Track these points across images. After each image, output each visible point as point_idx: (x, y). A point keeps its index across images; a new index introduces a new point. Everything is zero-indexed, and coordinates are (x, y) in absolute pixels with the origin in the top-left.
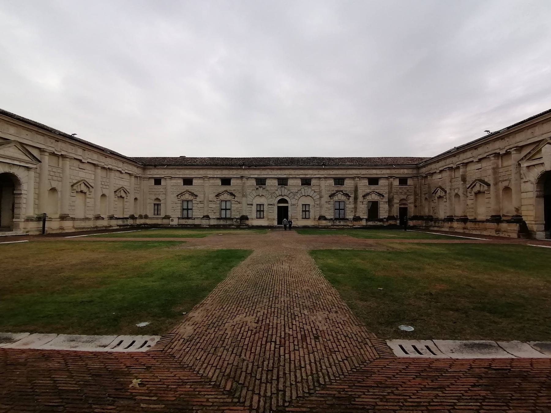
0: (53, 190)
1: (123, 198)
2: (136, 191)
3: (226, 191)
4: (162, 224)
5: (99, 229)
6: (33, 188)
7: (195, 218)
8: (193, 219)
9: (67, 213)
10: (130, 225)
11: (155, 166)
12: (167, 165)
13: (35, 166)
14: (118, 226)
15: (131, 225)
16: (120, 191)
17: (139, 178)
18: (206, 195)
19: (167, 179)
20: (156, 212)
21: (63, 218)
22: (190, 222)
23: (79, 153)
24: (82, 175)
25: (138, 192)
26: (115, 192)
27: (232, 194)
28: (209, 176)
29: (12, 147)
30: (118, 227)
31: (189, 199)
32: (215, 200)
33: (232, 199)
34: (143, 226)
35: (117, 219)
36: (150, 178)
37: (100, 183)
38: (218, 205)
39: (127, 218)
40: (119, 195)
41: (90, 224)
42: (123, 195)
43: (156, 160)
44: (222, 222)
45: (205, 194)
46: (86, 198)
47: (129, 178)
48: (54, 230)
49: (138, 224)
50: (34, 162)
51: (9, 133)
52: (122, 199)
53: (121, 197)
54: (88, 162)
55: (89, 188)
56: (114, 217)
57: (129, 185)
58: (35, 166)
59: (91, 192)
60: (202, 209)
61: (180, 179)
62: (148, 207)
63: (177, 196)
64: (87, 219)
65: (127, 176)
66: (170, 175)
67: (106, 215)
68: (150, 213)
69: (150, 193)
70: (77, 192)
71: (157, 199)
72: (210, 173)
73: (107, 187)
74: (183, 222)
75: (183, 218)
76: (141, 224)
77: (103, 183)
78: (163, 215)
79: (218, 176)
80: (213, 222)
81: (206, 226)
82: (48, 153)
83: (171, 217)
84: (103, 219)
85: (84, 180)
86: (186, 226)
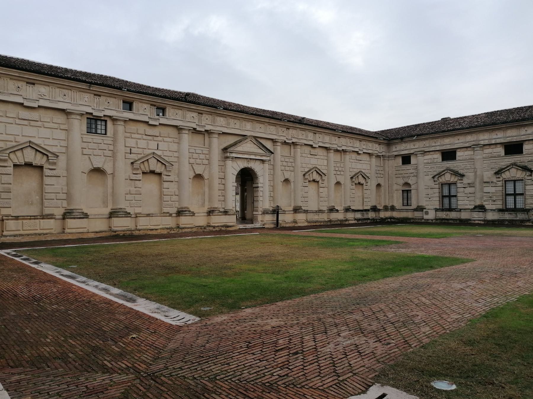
0: (287, 181)
1: (362, 184)
2: (379, 175)
3: (514, 165)
4: (413, 219)
5: (333, 223)
6: (268, 180)
7: (461, 209)
8: (458, 211)
9: (299, 205)
10: (371, 220)
11: (402, 139)
12: (418, 135)
13: (268, 158)
14: (355, 219)
15: (373, 219)
16: (358, 176)
17: (382, 159)
18: (478, 173)
19: (418, 156)
20: (405, 202)
21: (296, 210)
22: (453, 215)
23: (309, 137)
24: (314, 162)
25: (382, 176)
26: (352, 178)
27: (525, 168)
28: (482, 143)
29: (248, 142)
30: (356, 222)
31: (451, 181)
32: (495, 180)
33: (526, 177)
34: (389, 220)
35: (306, 212)
36: (396, 156)
37: (333, 168)
38: (500, 188)
39: (368, 210)
40: (357, 182)
41: (324, 217)
42: (362, 181)
43: (405, 130)
44: (507, 216)
45: (475, 172)
46: (319, 187)
47: (368, 159)
48: (287, 223)
49: (382, 218)
50: (268, 154)
51: (246, 129)
52: (360, 187)
53: (359, 183)
54: (319, 146)
55: (321, 175)
56: (351, 209)
57: (369, 168)
58: (268, 158)
59: (323, 180)
60: (472, 195)
61: (437, 152)
62: (395, 195)
63: (433, 177)
64: (320, 211)
65: (366, 157)
66: (423, 149)
67: (341, 206)
68: (398, 203)
69: (397, 176)
70: (309, 181)
71: (407, 184)
72: (484, 138)
73: (342, 173)
74: (442, 215)
75: (443, 210)
76: (387, 218)
77: (337, 169)
78: (414, 206)
79: (498, 141)
80: (491, 216)
81: (479, 222)
83: (425, 209)
84: (337, 211)
85: (316, 167)
86: (446, 221)
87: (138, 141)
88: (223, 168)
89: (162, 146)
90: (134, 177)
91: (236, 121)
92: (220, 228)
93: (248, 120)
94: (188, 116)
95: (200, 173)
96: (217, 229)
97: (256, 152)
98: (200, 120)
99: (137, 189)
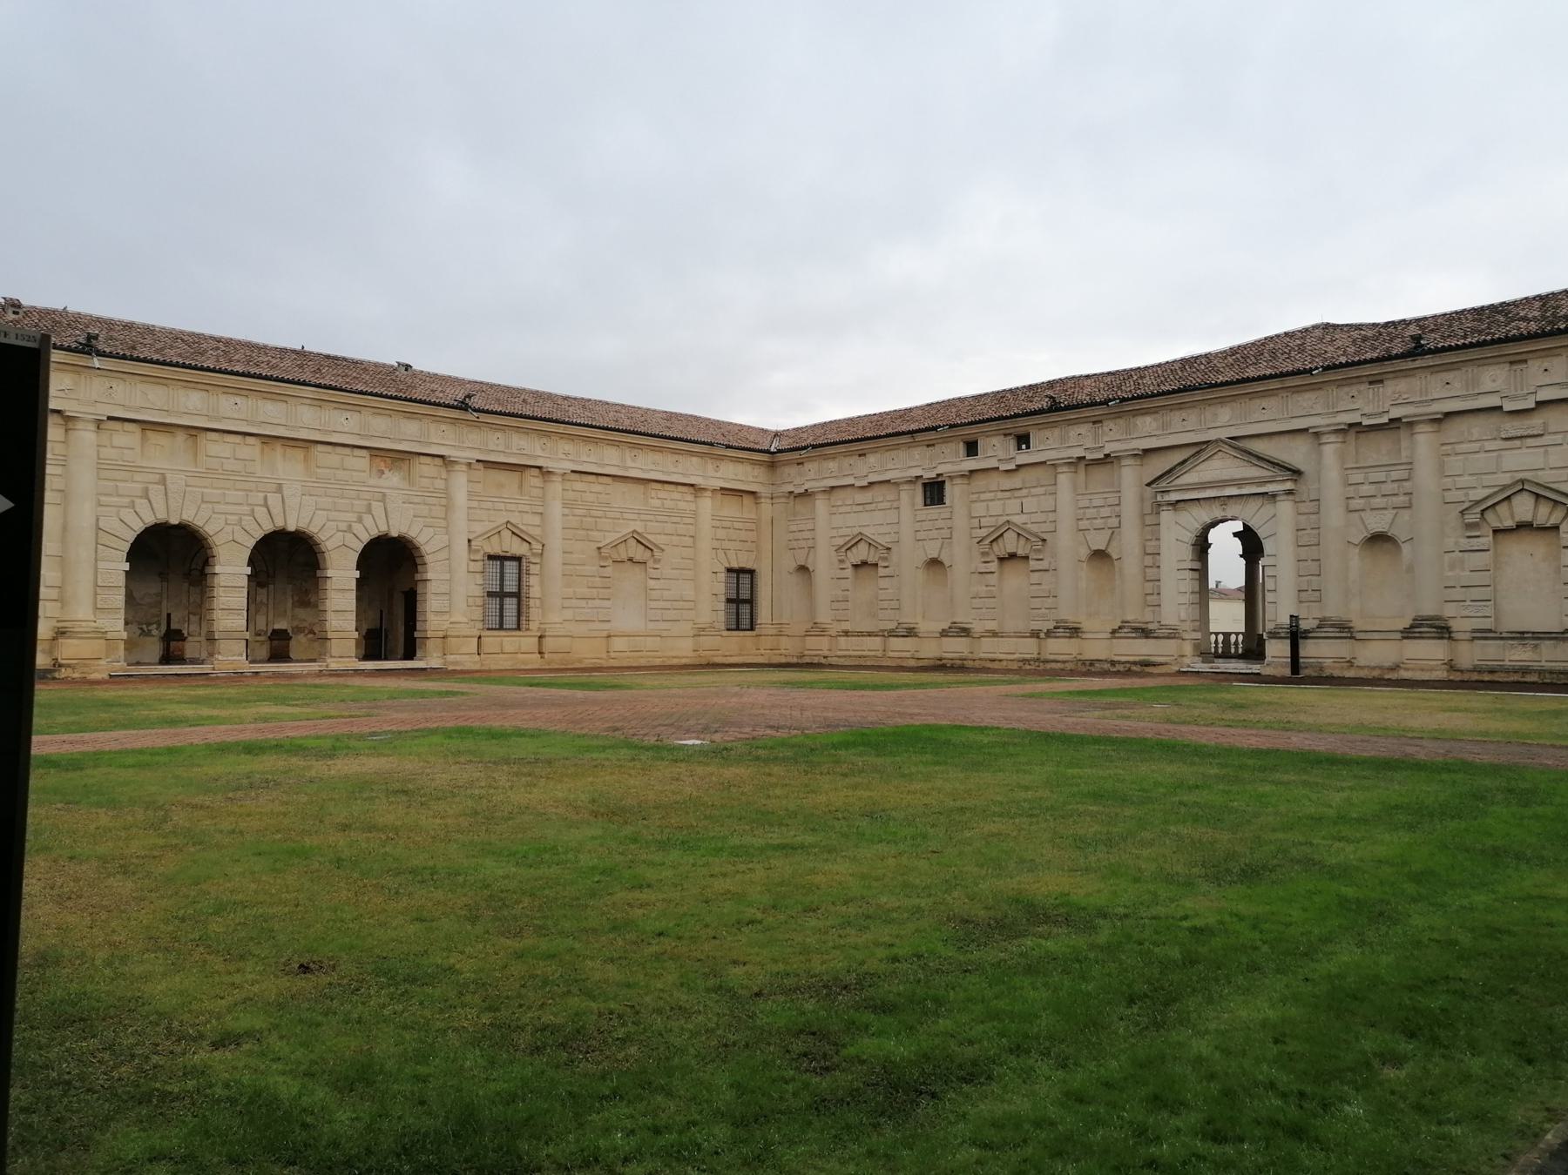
13: (1289, 485)
29: (1216, 457)
82: (1329, 433)
87: (990, 504)
88: (1151, 529)
89: (1030, 504)
90: (983, 568)
91: (1184, 414)
92: (1128, 665)
93: (1219, 400)
95: (1101, 548)
96: (1120, 668)
98: (1096, 438)
99: (989, 588)
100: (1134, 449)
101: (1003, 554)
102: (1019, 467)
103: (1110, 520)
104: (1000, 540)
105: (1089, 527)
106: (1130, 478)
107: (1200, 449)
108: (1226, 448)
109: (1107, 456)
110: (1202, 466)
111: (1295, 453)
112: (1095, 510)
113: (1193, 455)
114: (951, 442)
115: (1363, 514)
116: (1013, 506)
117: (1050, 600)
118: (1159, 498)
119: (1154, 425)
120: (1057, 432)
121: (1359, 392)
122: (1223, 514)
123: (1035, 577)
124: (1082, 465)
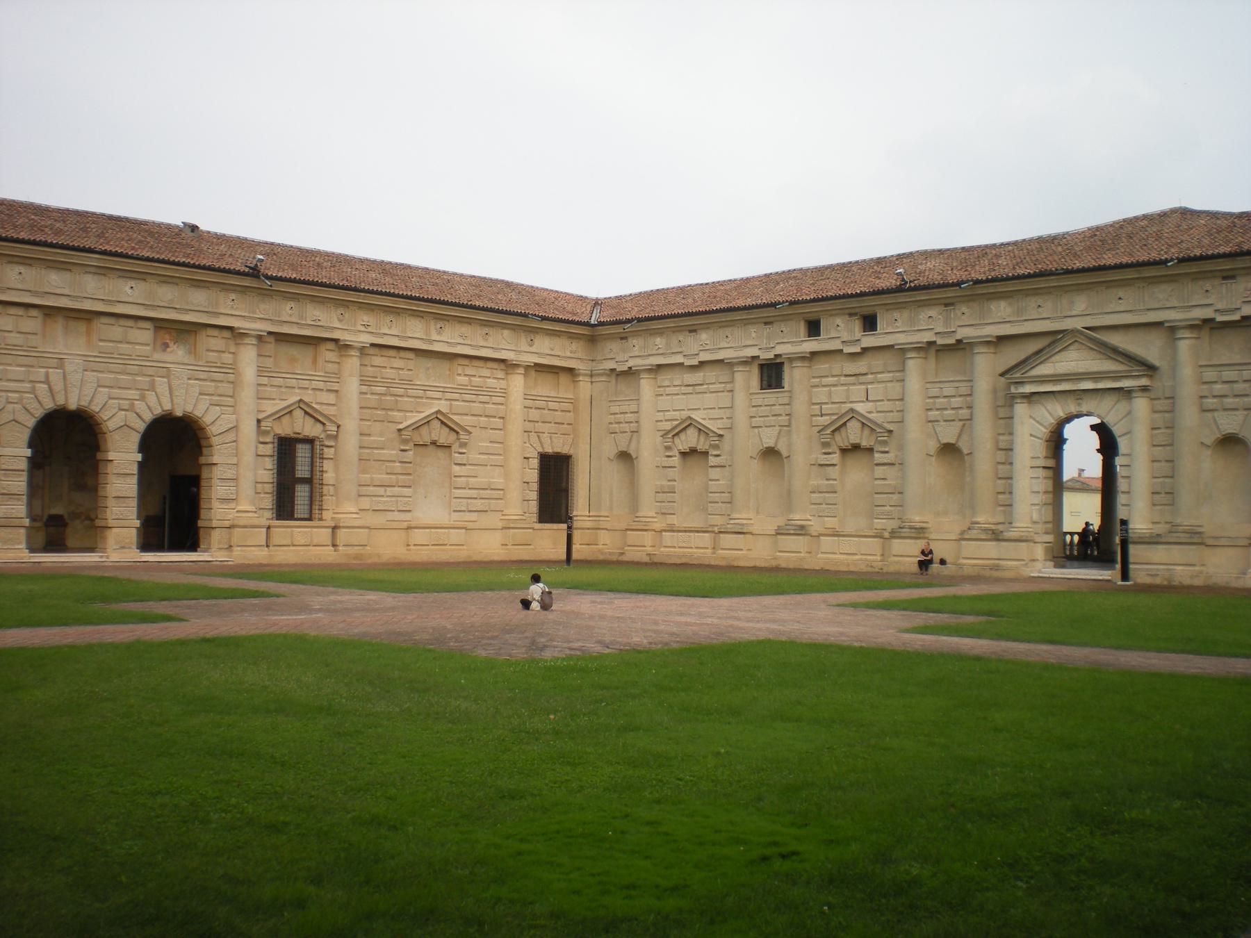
13: (1144, 381)
29: (1072, 347)
87: (833, 389)
90: (823, 459)
94: (921, 317)
97: (1095, 369)
98: (947, 321)
100: (987, 336)
101: (845, 444)
102: (865, 350)
103: (961, 412)
104: (843, 430)
105: (939, 418)
106: (985, 367)
107: (1055, 340)
108: (1081, 339)
109: (959, 341)
110: (1057, 357)
111: (1149, 348)
112: (946, 400)
113: (1049, 345)
114: (791, 320)
115: (1216, 414)
116: (857, 391)
117: (895, 497)
118: (1013, 390)
119: (1009, 310)
120: (906, 314)
121: (1213, 286)
122: (1078, 409)
123: (880, 471)
124: (932, 351)
